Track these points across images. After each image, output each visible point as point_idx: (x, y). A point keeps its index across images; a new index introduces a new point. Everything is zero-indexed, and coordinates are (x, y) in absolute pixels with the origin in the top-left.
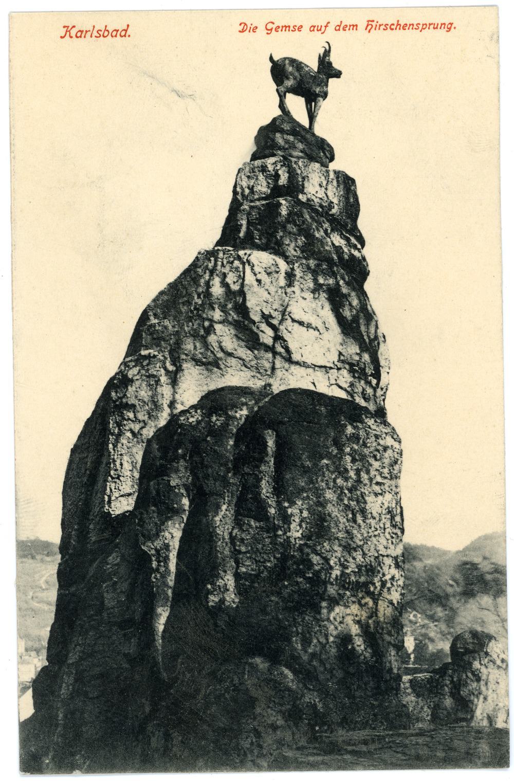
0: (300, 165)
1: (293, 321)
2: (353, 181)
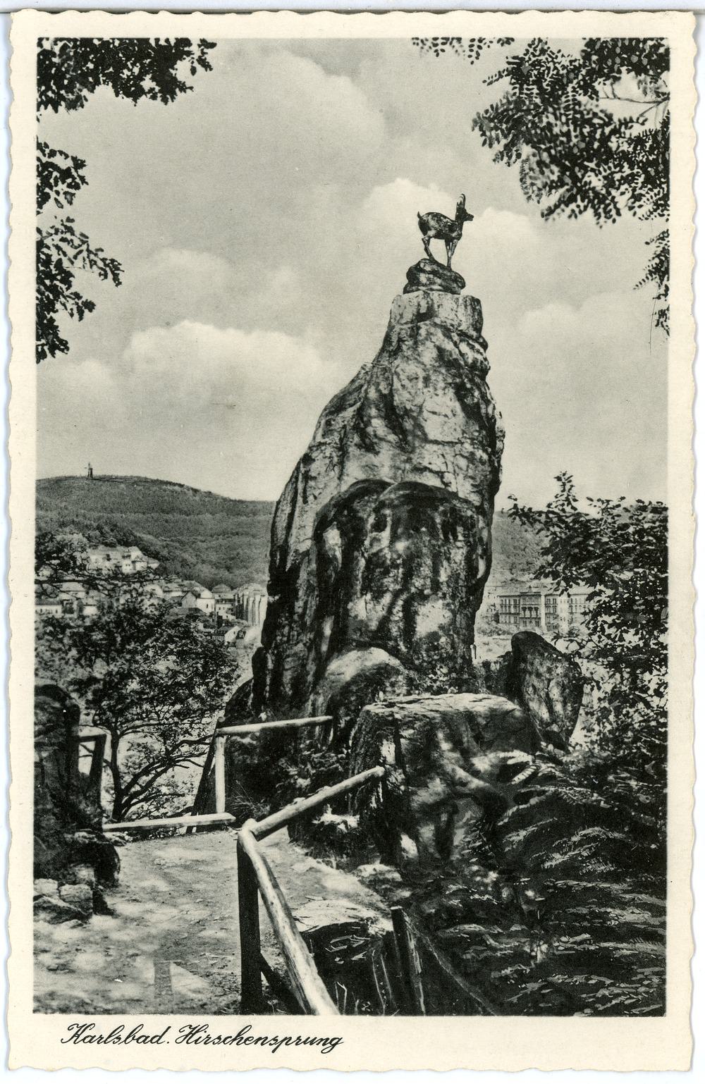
0: (435, 295)
2: (478, 301)
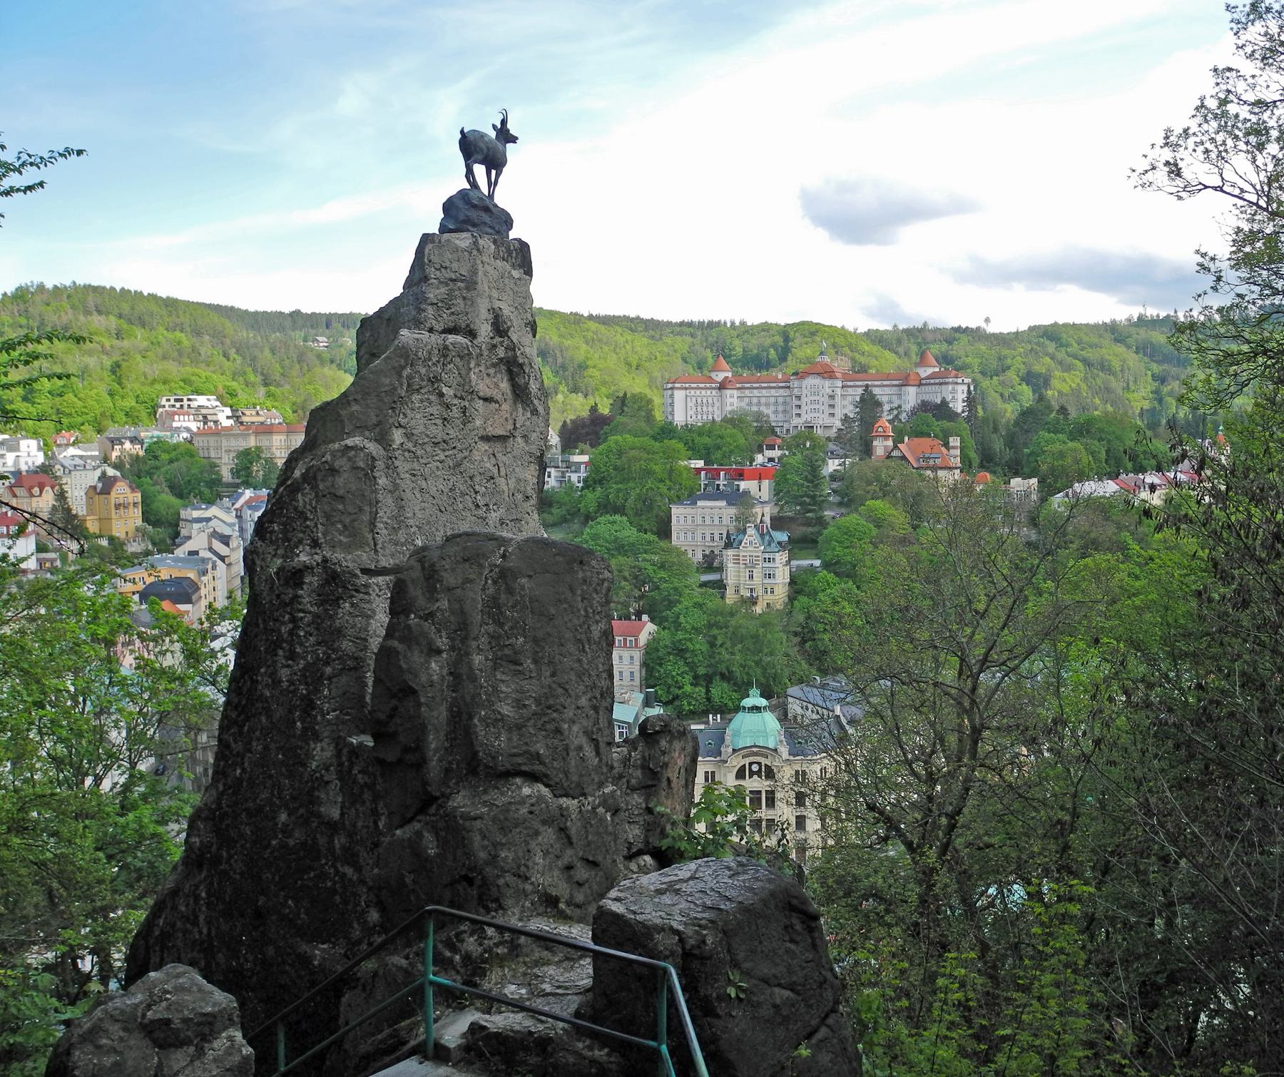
1: (480, 398)
